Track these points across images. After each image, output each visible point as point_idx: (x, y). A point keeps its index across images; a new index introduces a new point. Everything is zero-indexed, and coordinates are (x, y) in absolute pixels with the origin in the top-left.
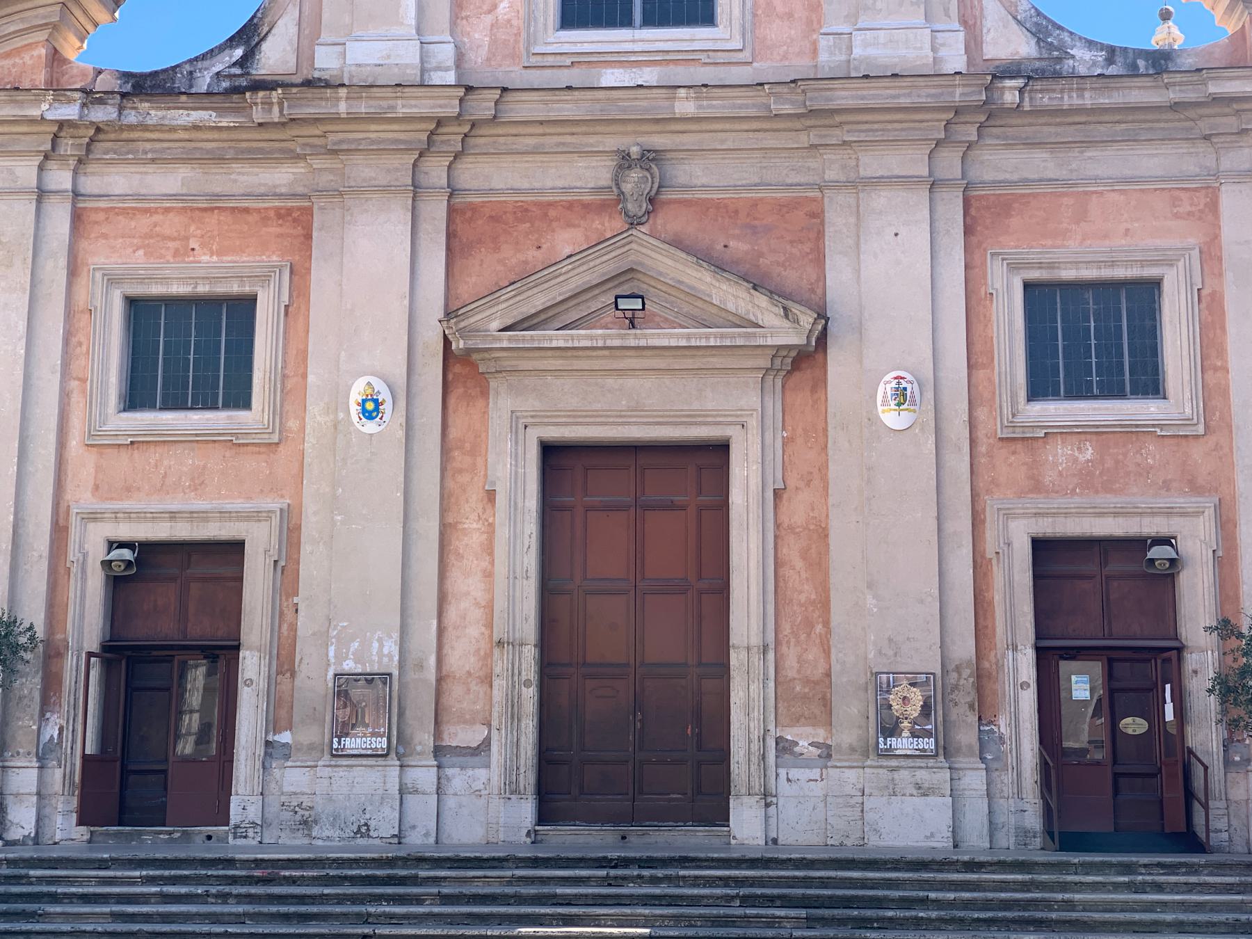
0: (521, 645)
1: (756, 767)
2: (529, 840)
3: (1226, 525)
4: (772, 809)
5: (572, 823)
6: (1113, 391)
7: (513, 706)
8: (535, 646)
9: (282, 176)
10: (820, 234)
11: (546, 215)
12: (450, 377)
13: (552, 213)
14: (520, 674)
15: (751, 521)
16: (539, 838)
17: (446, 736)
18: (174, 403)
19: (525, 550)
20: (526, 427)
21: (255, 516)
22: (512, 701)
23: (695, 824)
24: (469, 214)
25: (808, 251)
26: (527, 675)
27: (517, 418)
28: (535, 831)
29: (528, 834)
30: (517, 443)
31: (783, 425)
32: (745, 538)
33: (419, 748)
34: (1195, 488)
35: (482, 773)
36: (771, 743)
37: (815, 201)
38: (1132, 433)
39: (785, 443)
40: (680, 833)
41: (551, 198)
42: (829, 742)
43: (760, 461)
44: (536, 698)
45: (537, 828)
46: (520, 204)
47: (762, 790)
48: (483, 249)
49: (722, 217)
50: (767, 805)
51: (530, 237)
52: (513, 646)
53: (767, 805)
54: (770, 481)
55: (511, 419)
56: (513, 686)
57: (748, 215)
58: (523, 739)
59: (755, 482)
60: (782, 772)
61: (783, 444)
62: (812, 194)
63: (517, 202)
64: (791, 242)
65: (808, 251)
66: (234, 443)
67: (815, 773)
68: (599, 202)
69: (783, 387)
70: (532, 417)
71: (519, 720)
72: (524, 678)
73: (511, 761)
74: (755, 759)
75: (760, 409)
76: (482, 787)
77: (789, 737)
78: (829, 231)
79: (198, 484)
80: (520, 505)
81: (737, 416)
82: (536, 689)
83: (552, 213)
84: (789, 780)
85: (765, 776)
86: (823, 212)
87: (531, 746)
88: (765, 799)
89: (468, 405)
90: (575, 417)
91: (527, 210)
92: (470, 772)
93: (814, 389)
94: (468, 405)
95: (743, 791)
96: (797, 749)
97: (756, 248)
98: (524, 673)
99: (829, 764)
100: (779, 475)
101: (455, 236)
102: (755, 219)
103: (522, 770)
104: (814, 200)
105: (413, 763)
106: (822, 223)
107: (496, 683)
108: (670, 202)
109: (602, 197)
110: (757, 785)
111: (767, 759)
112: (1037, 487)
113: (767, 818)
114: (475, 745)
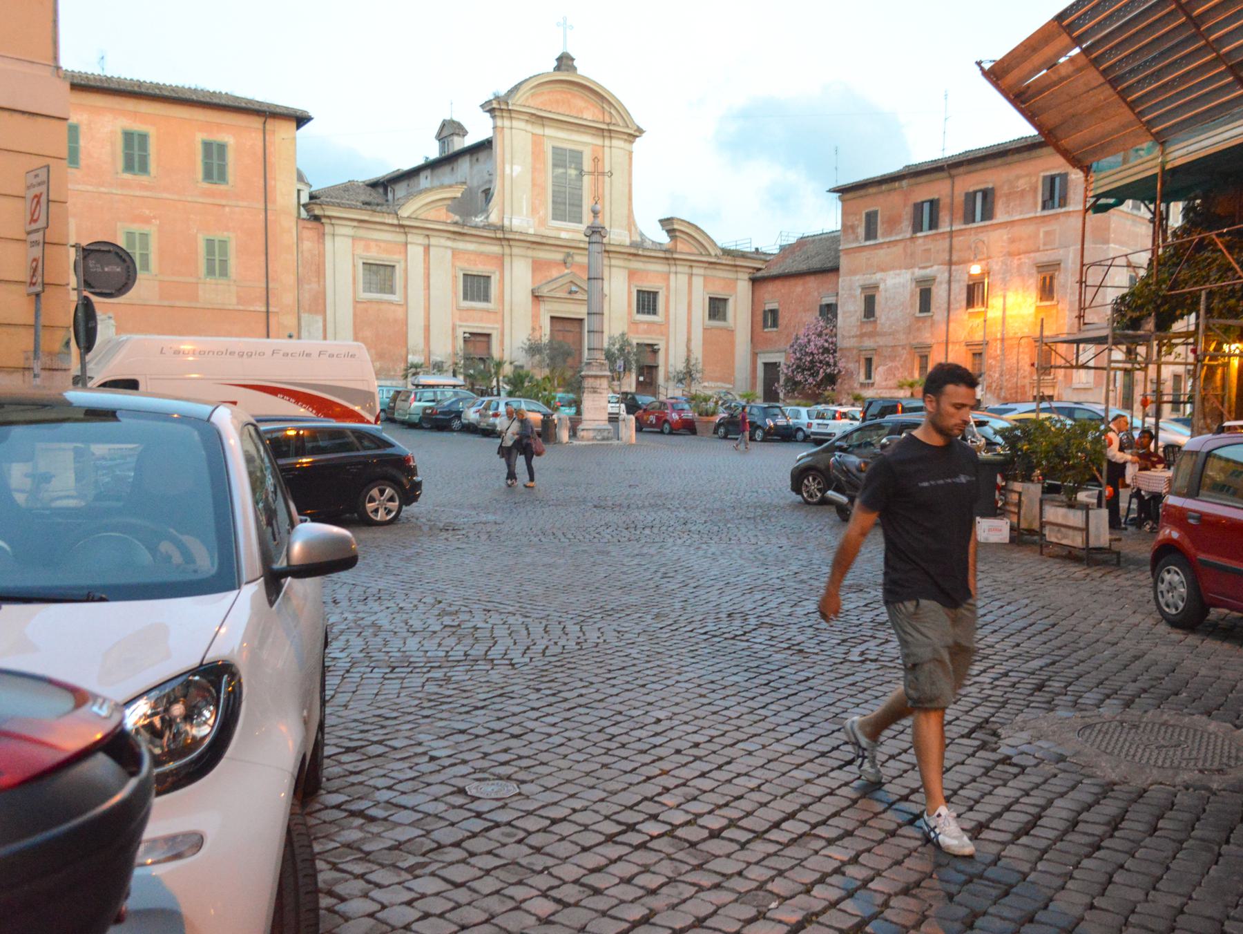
3: (667, 343)
6: (649, 313)
9: (495, 249)
18: (472, 299)
21: (493, 328)
34: (662, 334)
38: (653, 323)
66: (488, 311)
79: (481, 320)
90: (557, 311)
112: (637, 332)
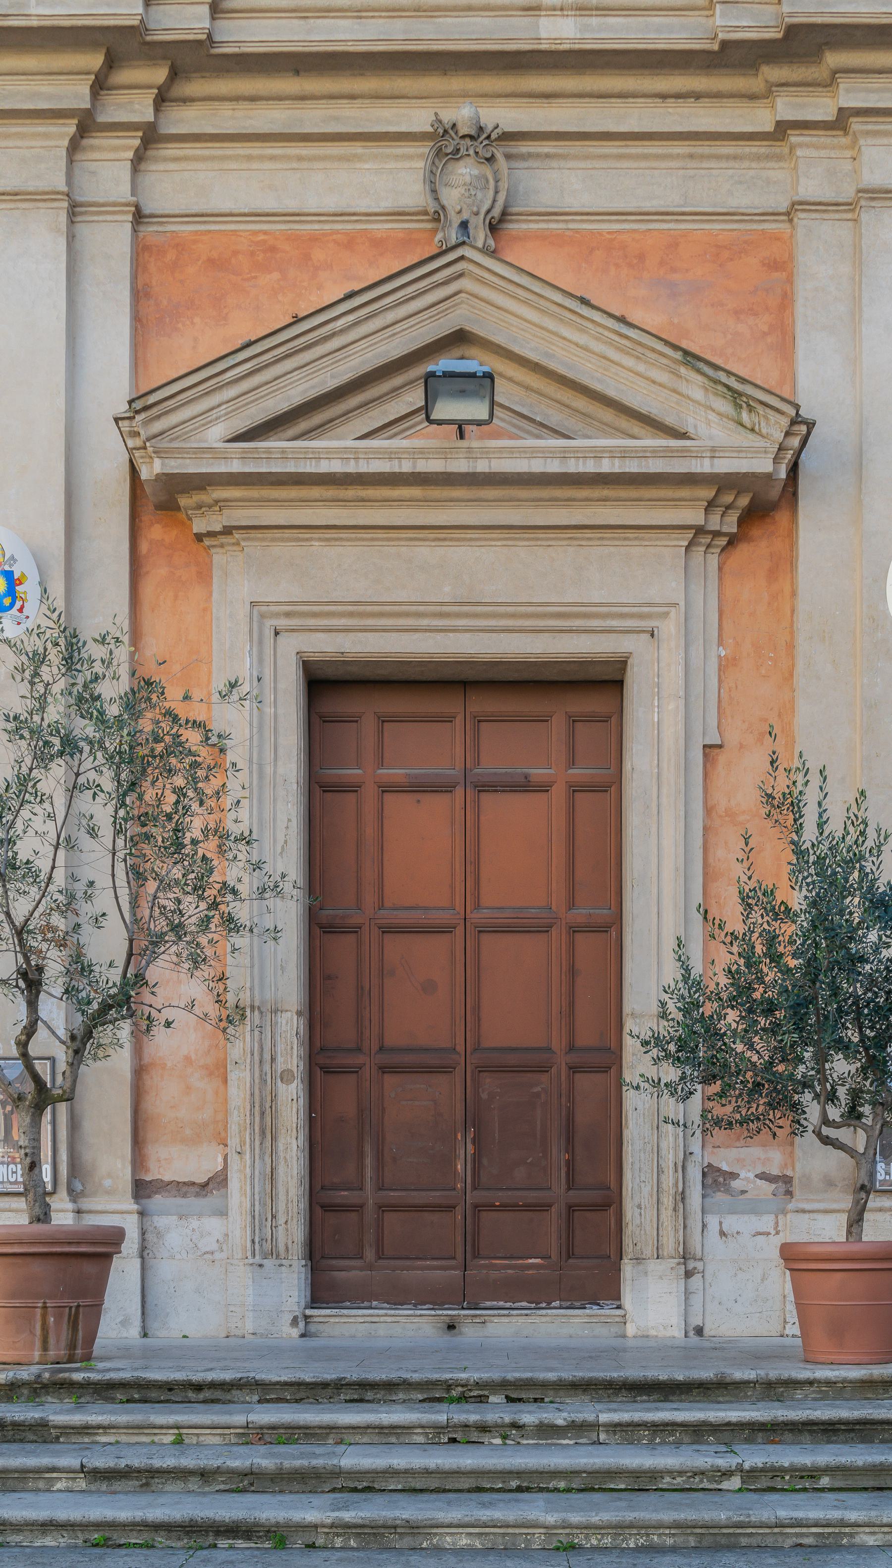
0: (275, 1011)
1: (670, 1212)
2: (295, 1332)
4: (696, 1280)
5: (366, 1304)
7: (263, 1113)
8: (299, 1013)
10: (786, 301)
11: (307, 257)
12: (144, 547)
13: (318, 255)
14: (273, 1059)
15: (664, 800)
16: (313, 1328)
17: (152, 1164)
19: (279, 850)
20: (277, 633)
22: (261, 1106)
23: (565, 1304)
24: (171, 256)
25: (765, 328)
26: (286, 1062)
27: (262, 616)
28: (306, 1317)
29: (295, 1322)
30: (261, 661)
31: (720, 635)
32: (654, 829)
33: (107, 1183)
35: (213, 1225)
36: (695, 1174)
37: (778, 239)
39: (724, 666)
40: (544, 1319)
41: (316, 227)
42: (789, 1173)
43: (682, 693)
44: (301, 1101)
45: (309, 1312)
46: (262, 237)
47: (681, 1249)
48: (197, 320)
49: (617, 266)
50: (688, 1274)
51: (280, 297)
52: (261, 1013)
53: (688, 1274)
54: (698, 728)
55: (251, 618)
56: (263, 1081)
57: (662, 263)
58: (281, 1170)
59: (672, 731)
60: (713, 1221)
61: (720, 670)
62: (773, 226)
63: (255, 233)
64: (737, 313)
65: (765, 328)
67: (766, 1222)
68: (401, 235)
69: (720, 569)
70: (288, 615)
71: (274, 1139)
72: (280, 1066)
73: (263, 1204)
74: (668, 1201)
75: (682, 604)
76: (214, 1246)
77: (725, 1167)
78: (803, 290)
80: (269, 770)
81: (641, 616)
82: (301, 1086)
83: (318, 255)
84: (722, 1234)
85: (685, 1227)
86: (791, 257)
87: (295, 1180)
88: (685, 1264)
89: (176, 597)
91: (273, 249)
92: (194, 1223)
93: (772, 574)
94: (176, 597)
95: (649, 1251)
96: (736, 1184)
97: (676, 321)
98: (280, 1059)
99: (791, 1206)
100: (713, 722)
101: (147, 295)
102: (673, 270)
103: (281, 1219)
104: (776, 238)
105: (99, 1208)
106: (790, 280)
107: (233, 1076)
108: (525, 237)
109: (406, 225)
110: (669, 1243)
111: (687, 1201)
113: (687, 1293)
114: (202, 1179)
